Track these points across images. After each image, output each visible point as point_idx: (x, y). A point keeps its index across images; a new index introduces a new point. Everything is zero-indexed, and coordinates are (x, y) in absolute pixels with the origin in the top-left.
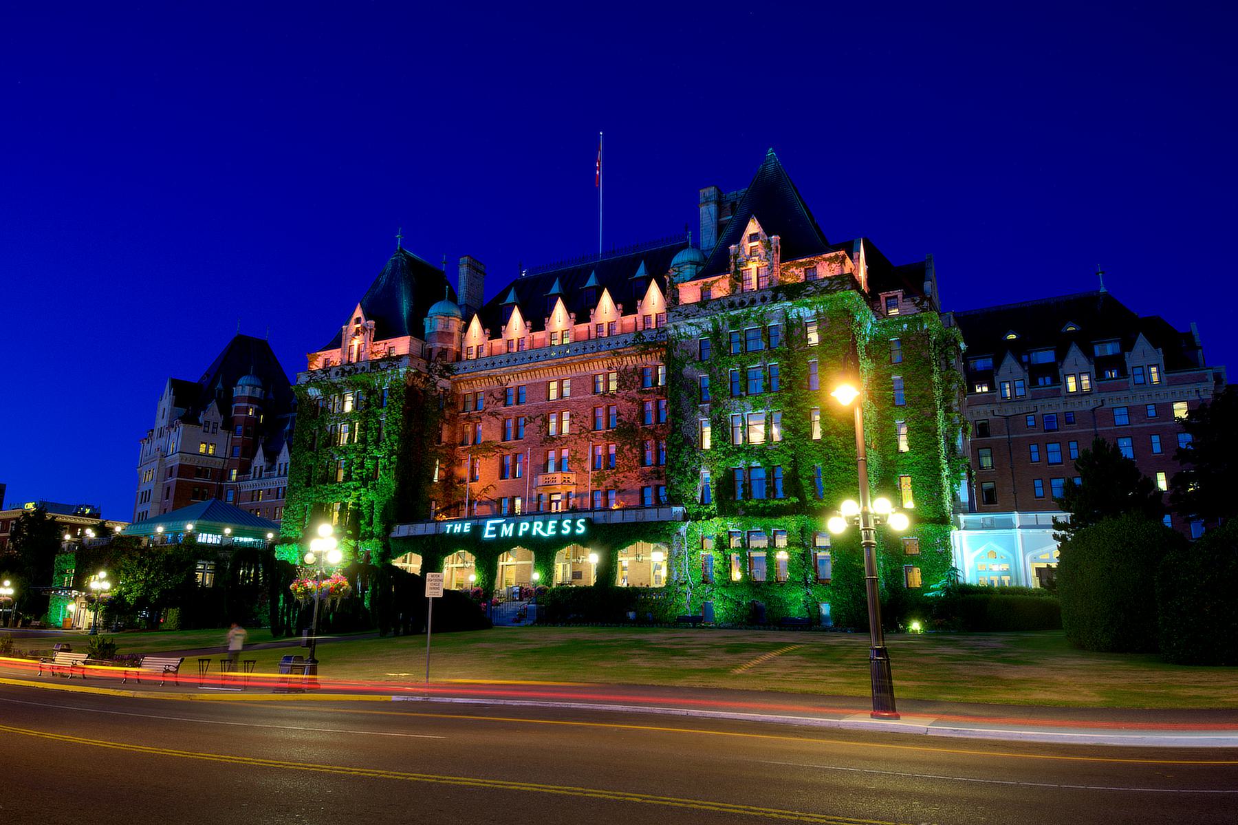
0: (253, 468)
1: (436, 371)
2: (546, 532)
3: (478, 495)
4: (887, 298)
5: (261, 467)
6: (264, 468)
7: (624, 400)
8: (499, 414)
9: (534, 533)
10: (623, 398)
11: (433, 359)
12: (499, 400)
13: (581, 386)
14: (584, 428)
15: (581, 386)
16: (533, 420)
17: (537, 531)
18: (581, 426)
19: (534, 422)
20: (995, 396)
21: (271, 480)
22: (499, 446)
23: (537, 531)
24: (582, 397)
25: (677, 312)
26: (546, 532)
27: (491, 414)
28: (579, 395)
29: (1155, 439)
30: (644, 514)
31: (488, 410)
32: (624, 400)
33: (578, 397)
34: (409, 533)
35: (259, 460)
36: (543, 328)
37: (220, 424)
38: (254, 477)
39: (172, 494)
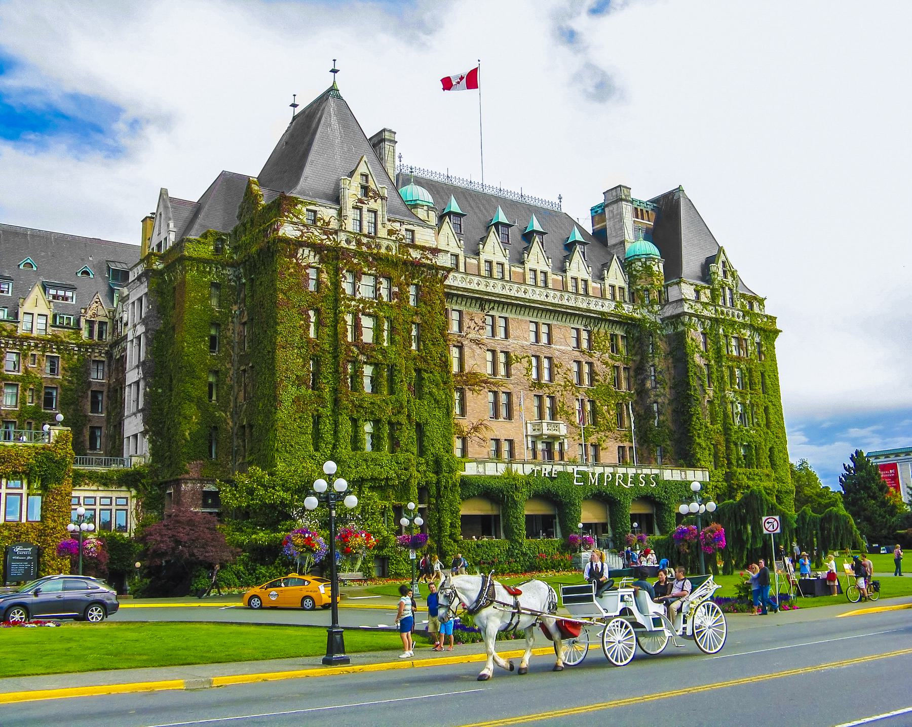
2: (627, 485)
10: (599, 360)
13: (562, 337)
14: (569, 381)
15: (562, 337)
17: (619, 482)
19: (520, 362)
22: (486, 382)
23: (619, 482)
25: (690, 304)
26: (627, 485)
30: (685, 474)
31: (470, 336)
34: (478, 472)
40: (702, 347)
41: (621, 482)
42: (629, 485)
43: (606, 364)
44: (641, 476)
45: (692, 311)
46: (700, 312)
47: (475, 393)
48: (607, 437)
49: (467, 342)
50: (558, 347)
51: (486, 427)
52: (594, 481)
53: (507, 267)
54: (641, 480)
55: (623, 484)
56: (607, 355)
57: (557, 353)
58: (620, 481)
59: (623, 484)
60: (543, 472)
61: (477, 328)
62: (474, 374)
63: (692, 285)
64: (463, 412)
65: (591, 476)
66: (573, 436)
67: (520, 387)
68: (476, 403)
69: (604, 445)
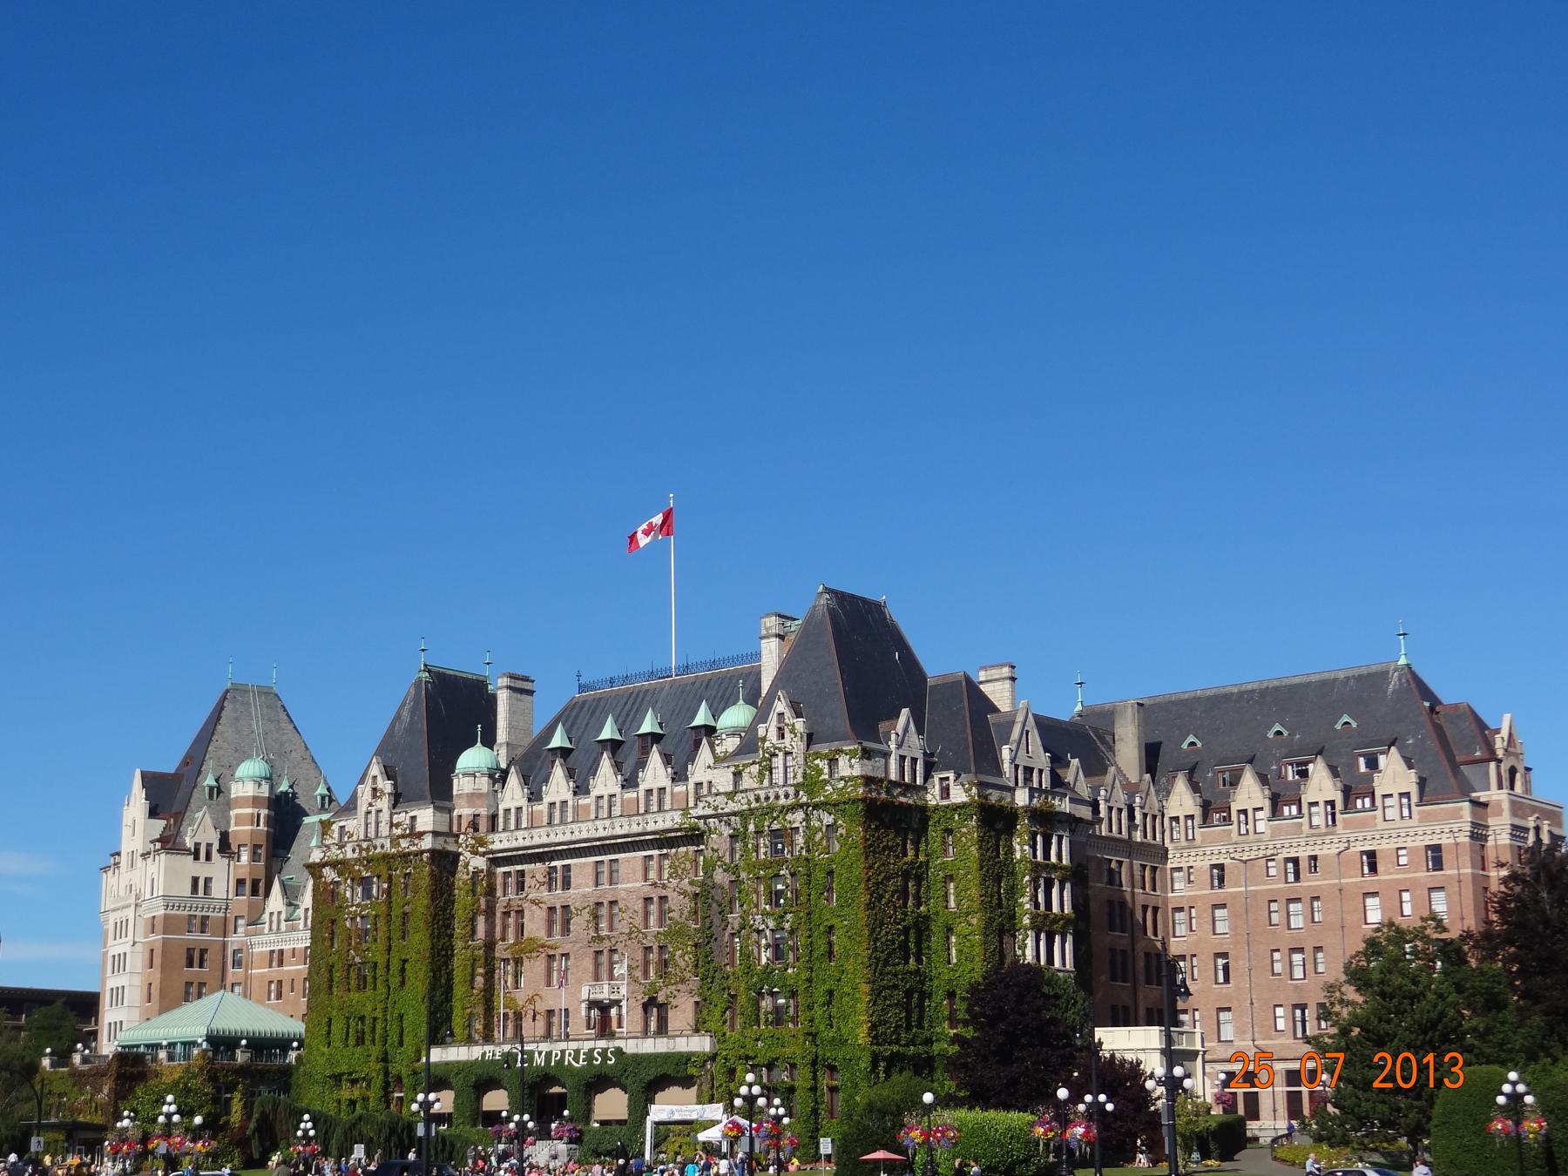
0: (266, 917)
1: (467, 847)
3: (523, 1007)
4: (941, 779)
5: (280, 913)
6: (283, 917)
7: (676, 893)
8: (541, 903)
9: (566, 1063)
10: (674, 890)
11: (463, 830)
12: (542, 884)
16: (579, 912)
17: (569, 1060)
18: (631, 923)
20: (1231, 830)
21: (294, 935)
23: (569, 1060)
24: (631, 885)
25: (706, 802)
27: (533, 902)
28: (628, 882)
29: (1406, 896)
32: (676, 893)
33: (629, 885)
35: (276, 901)
36: (587, 792)
37: (216, 846)
38: (270, 929)
39: (157, 960)
40: (727, 859)
41: (571, 1060)
42: (581, 1062)
43: (685, 893)
44: (595, 1053)
45: (710, 812)
46: (722, 809)
47: (532, 961)
48: (679, 991)
49: (526, 905)
50: (624, 886)
51: (541, 997)
52: (539, 1061)
53: (570, 803)
54: (596, 1055)
55: (573, 1063)
56: (687, 880)
57: (623, 894)
58: (570, 1058)
59: (573, 1063)
60: (488, 1054)
61: (538, 885)
62: (531, 939)
63: (728, 767)
64: (517, 985)
65: (536, 1053)
66: (635, 995)
67: (578, 945)
68: (532, 972)
69: (674, 1003)
